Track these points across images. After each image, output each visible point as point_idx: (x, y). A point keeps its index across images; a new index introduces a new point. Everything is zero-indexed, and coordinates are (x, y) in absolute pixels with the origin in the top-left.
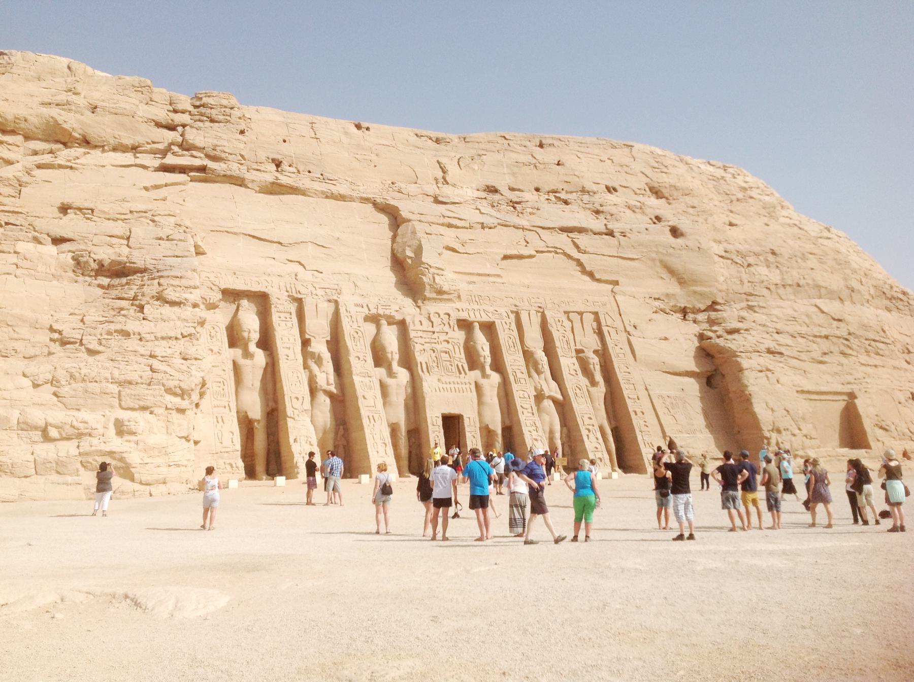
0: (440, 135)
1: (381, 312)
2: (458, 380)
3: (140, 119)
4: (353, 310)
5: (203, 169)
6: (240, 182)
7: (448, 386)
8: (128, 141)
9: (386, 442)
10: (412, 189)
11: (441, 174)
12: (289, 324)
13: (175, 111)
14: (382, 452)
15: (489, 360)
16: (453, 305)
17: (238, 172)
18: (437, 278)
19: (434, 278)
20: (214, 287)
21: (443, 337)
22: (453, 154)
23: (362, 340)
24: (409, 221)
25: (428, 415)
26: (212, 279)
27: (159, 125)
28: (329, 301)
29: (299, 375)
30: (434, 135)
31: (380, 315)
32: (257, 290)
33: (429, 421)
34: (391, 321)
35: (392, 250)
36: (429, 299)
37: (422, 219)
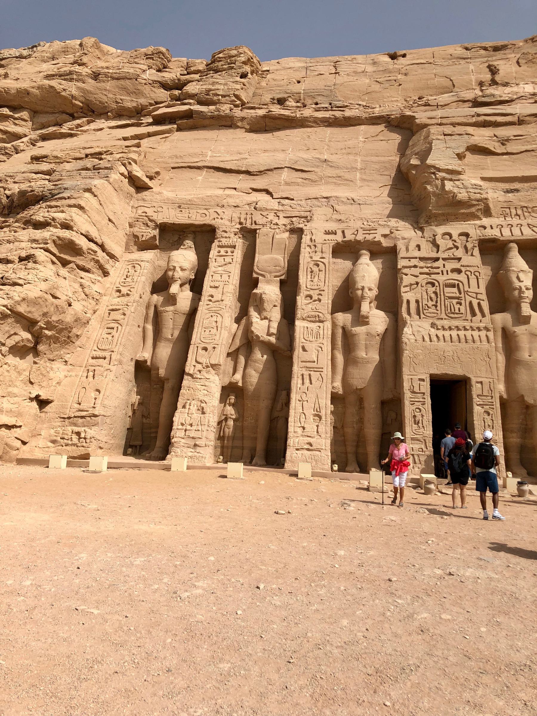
0: (500, 43)
1: (360, 237)
2: (467, 324)
3: (144, 81)
4: (320, 237)
5: (189, 115)
6: (226, 123)
7: (447, 333)
8: (129, 102)
9: (323, 414)
10: (445, 98)
11: (489, 76)
12: (228, 259)
13: (188, 74)
14: (311, 427)
15: (529, 294)
16: (478, 222)
17: (228, 111)
18: (449, 186)
19: (443, 185)
20: (150, 223)
21: (451, 265)
22: (513, 55)
23: (322, 275)
24: (426, 126)
25: (406, 377)
26: (150, 212)
27: (165, 86)
28: (292, 231)
29: (219, 319)
30: (488, 44)
31: (358, 242)
32: (202, 223)
33: (406, 385)
34: (376, 251)
35: (399, 166)
36: (436, 216)
37: (443, 122)
